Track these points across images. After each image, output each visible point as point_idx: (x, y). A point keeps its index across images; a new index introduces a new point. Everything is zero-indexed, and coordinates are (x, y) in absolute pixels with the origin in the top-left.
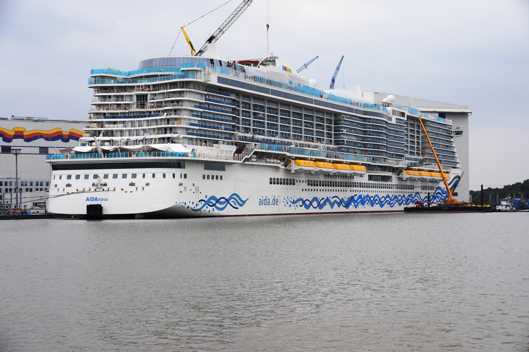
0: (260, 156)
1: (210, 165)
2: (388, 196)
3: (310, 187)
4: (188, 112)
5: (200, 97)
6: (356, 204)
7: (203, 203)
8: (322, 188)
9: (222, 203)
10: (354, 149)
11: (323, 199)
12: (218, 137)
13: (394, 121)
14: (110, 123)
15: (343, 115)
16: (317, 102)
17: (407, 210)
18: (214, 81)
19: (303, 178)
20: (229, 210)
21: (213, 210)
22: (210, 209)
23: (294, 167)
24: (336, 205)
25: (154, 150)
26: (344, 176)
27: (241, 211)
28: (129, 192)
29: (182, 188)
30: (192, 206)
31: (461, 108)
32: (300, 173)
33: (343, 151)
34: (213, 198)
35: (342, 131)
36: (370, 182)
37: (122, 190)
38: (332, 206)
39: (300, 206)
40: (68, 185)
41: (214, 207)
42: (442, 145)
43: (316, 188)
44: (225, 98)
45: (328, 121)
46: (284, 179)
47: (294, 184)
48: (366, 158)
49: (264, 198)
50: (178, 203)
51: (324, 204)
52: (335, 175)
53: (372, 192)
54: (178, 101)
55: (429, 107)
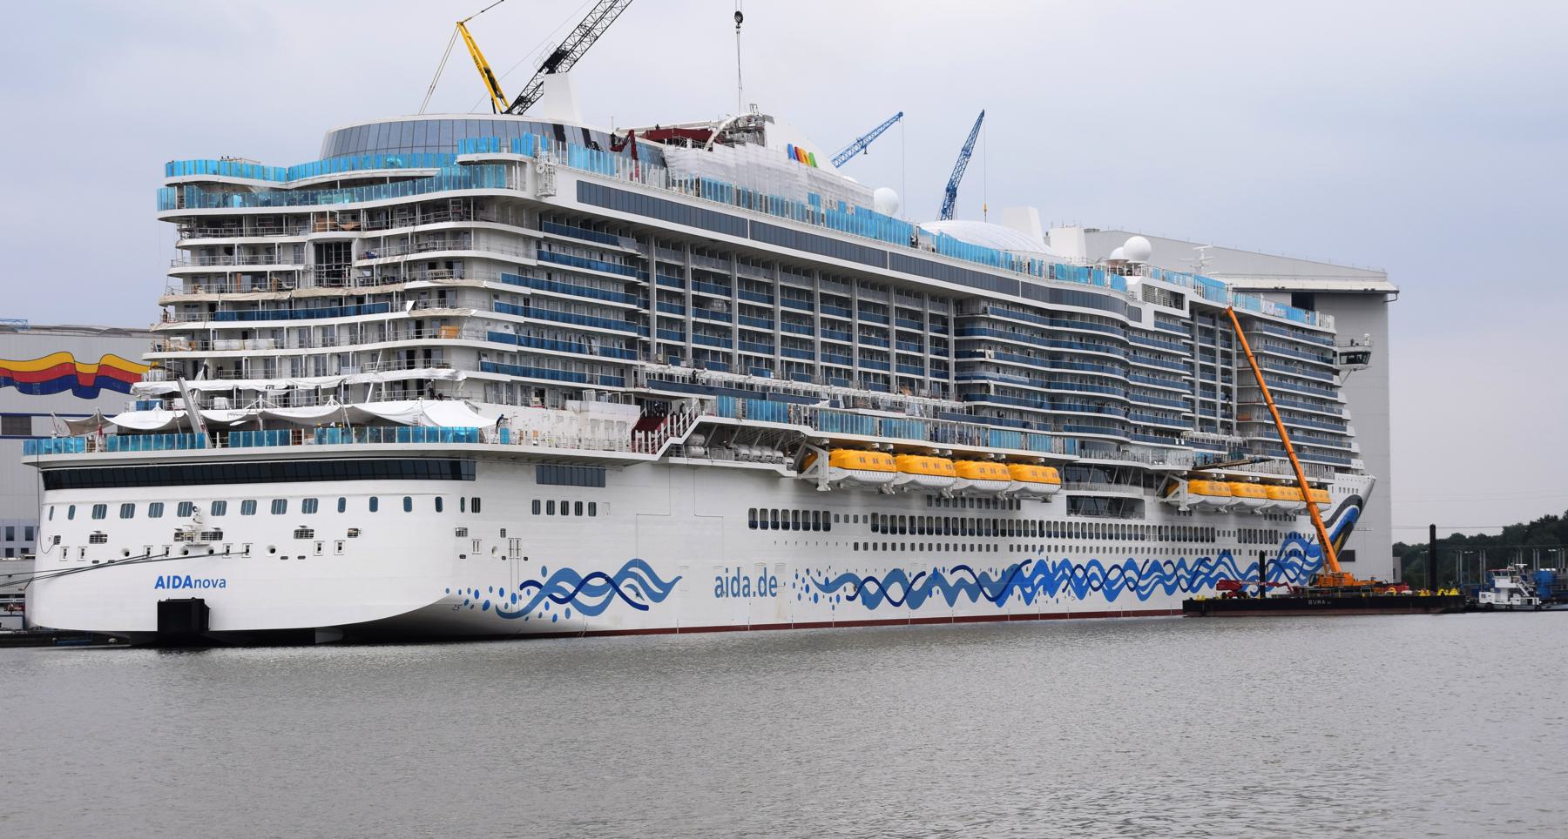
0: (717, 437)
1: (554, 469)
2: (1131, 564)
3: (879, 538)
4: (485, 299)
5: (521, 248)
6: (1029, 590)
7: (535, 591)
8: (917, 539)
9: (595, 592)
10: (1021, 412)
11: (923, 574)
12: (581, 379)
13: (1148, 323)
14: (229, 334)
15: (983, 304)
16: (900, 262)
17: (1194, 609)
18: (565, 196)
20: (619, 615)
21: (568, 613)
22: (558, 610)
23: (827, 471)
24: (963, 594)
25: (375, 421)
26: (987, 501)
27: (659, 615)
28: (293, 557)
29: (465, 544)
30: (497, 601)
31: (1363, 279)
32: (846, 492)
33: (984, 420)
34: (566, 574)
35: (983, 355)
36: (1074, 519)
37: (273, 551)
38: (951, 596)
39: (850, 599)
40: (98, 538)
41: (569, 605)
42: (1305, 398)
43: (898, 538)
44: (603, 252)
45: (936, 322)
46: (796, 513)
47: (827, 528)
48: (1059, 442)
50: (453, 591)
51: (926, 590)
52: (960, 499)
53: (1077, 552)
54: (449, 263)
55: (1262, 276)
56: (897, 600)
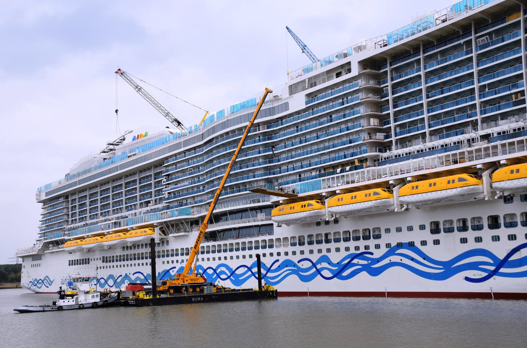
3: (105, 264)
8: (119, 263)
9: (40, 284)
10: (193, 197)
11: (121, 276)
19: (98, 255)
32: (94, 251)
34: (36, 280)
39: (95, 285)
47: (89, 263)
49: (65, 278)
56: (111, 285)
